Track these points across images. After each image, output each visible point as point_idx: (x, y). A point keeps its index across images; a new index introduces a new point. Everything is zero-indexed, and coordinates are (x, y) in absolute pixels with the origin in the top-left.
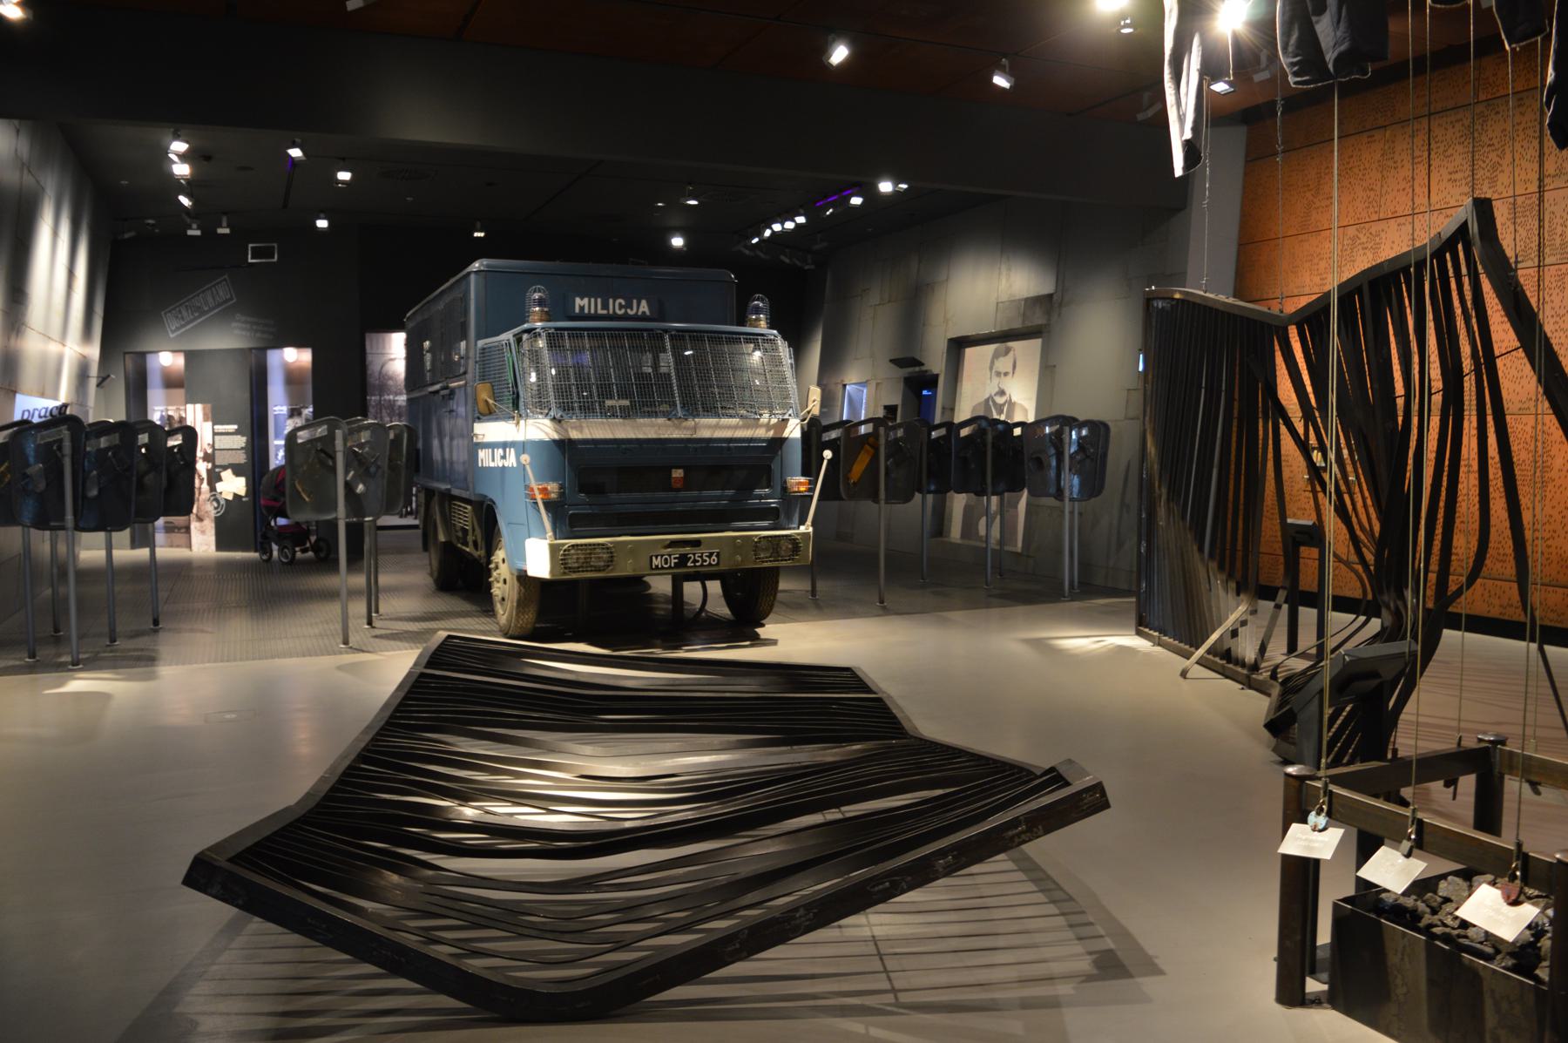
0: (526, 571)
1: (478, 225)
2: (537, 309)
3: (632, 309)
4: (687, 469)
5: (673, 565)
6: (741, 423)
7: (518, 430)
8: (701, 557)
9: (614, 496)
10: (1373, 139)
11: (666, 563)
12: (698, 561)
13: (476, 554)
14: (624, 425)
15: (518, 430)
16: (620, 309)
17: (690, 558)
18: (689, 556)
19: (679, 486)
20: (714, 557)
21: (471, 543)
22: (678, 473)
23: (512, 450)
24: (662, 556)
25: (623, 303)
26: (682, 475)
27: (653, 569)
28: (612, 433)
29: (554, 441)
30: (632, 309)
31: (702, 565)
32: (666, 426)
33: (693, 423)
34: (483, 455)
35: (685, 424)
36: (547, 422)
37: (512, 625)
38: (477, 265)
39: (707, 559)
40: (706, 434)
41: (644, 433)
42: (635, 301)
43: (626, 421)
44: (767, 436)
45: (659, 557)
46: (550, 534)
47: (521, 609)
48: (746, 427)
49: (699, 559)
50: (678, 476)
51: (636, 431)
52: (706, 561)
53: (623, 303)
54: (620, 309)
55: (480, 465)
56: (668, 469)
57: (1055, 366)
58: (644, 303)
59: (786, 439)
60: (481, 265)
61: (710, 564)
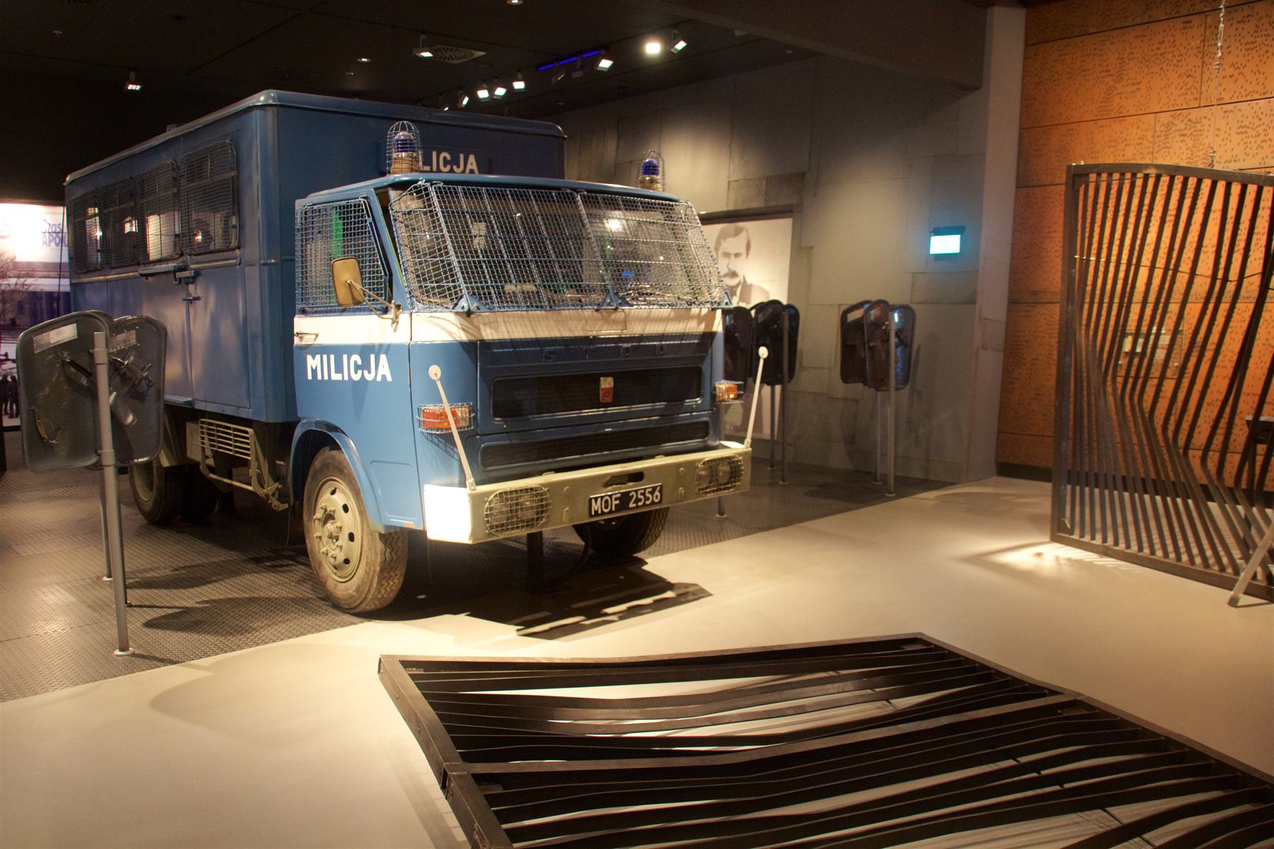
0: (424, 533)
1: (132, 75)
2: (404, 154)
4: (617, 377)
5: (613, 509)
6: (672, 314)
7: (395, 330)
8: (643, 494)
9: (536, 418)
10: (1191, 25)
13: (262, 492)
14: (547, 318)
15: (395, 330)
16: (445, 166)
17: (633, 496)
18: (631, 494)
19: (609, 400)
20: (657, 493)
21: (254, 480)
22: (607, 383)
23: (383, 358)
25: (449, 158)
26: (612, 385)
27: (591, 516)
28: (534, 331)
29: (462, 344)
31: (644, 505)
33: (623, 314)
34: (312, 362)
35: (614, 316)
36: (450, 316)
37: (370, 596)
38: (262, 98)
39: (650, 496)
40: (636, 329)
41: (571, 331)
42: (462, 156)
43: (550, 314)
44: (699, 330)
45: (599, 500)
46: (470, 480)
47: (385, 574)
48: (678, 318)
49: (642, 497)
50: (608, 386)
51: (562, 329)
52: (648, 499)
53: (449, 158)
54: (445, 166)
55: (310, 377)
56: (595, 379)
57: (812, 248)
58: (472, 159)
60: (268, 97)
61: (653, 503)
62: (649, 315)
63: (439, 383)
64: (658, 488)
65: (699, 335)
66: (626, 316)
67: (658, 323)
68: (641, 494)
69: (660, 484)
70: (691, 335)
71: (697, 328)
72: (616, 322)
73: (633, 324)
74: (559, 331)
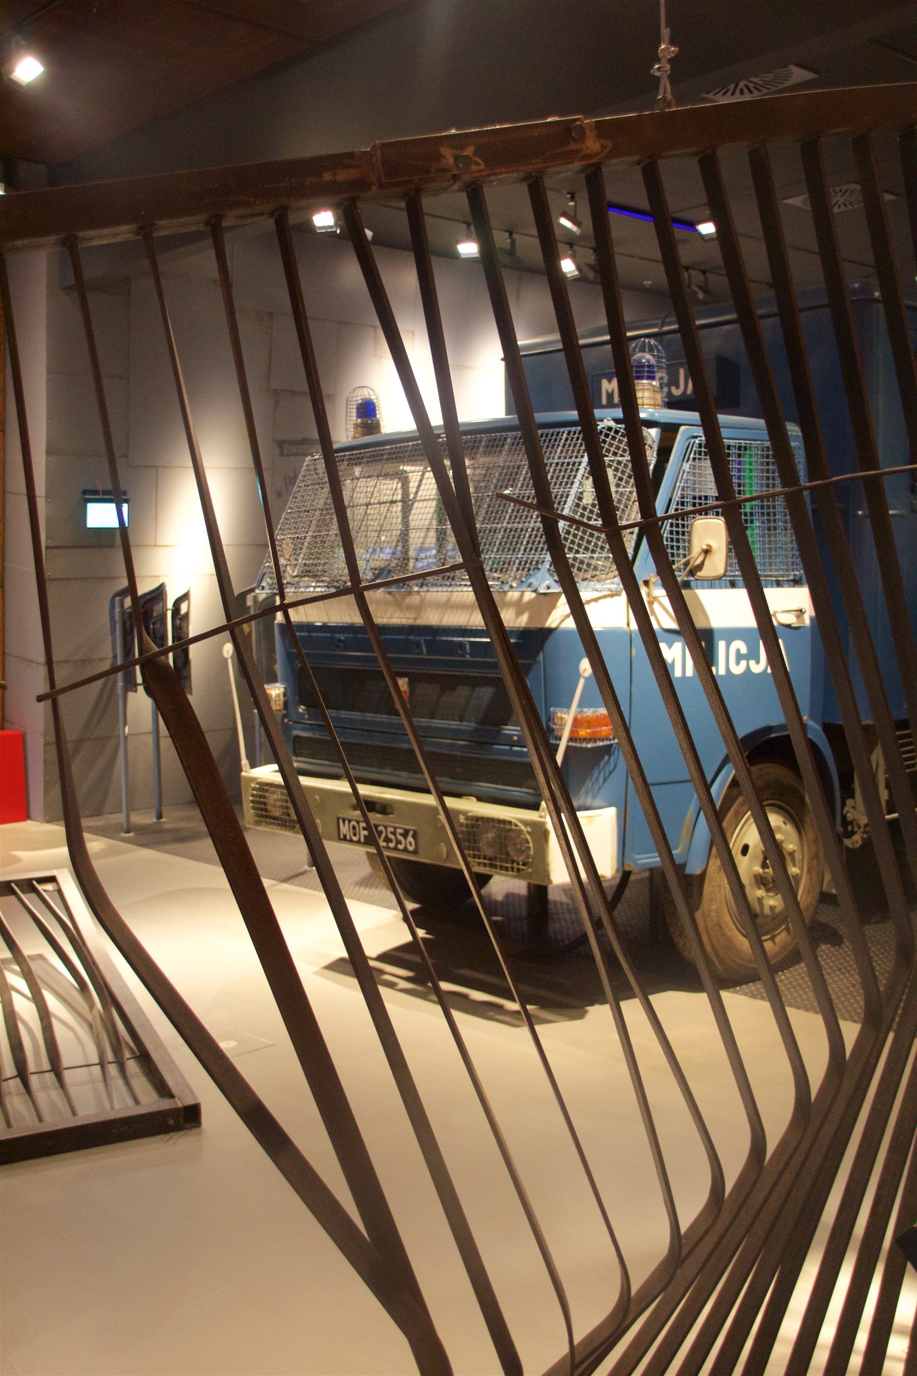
3: (678, 387)
4: (414, 680)
8: (394, 833)
11: (355, 835)
12: (391, 841)
20: (410, 839)
24: (350, 821)
28: (328, 615)
30: (678, 387)
32: (386, 603)
33: (418, 598)
40: (432, 618)
44: (517, 625)
52: (400, 843)
59: (550, 631)
61: (405, 850)
62: (449, 600)
63: (230, 661)
64: (411, 833)
65: (518, 631)
66: (422, 600)
67: (460, 611)
68: (392, 833)
69: (414, 828)
70: (471, 630)
71: (515, 621)
72: (409, 608)
73: (429, 611)
74: (350, 616)
